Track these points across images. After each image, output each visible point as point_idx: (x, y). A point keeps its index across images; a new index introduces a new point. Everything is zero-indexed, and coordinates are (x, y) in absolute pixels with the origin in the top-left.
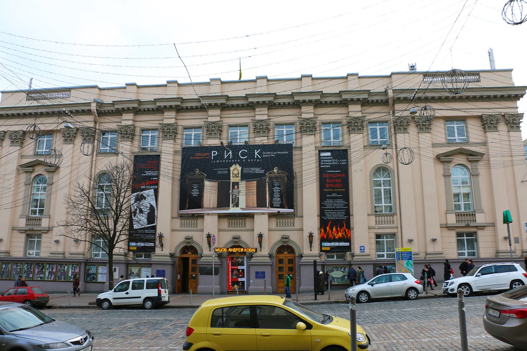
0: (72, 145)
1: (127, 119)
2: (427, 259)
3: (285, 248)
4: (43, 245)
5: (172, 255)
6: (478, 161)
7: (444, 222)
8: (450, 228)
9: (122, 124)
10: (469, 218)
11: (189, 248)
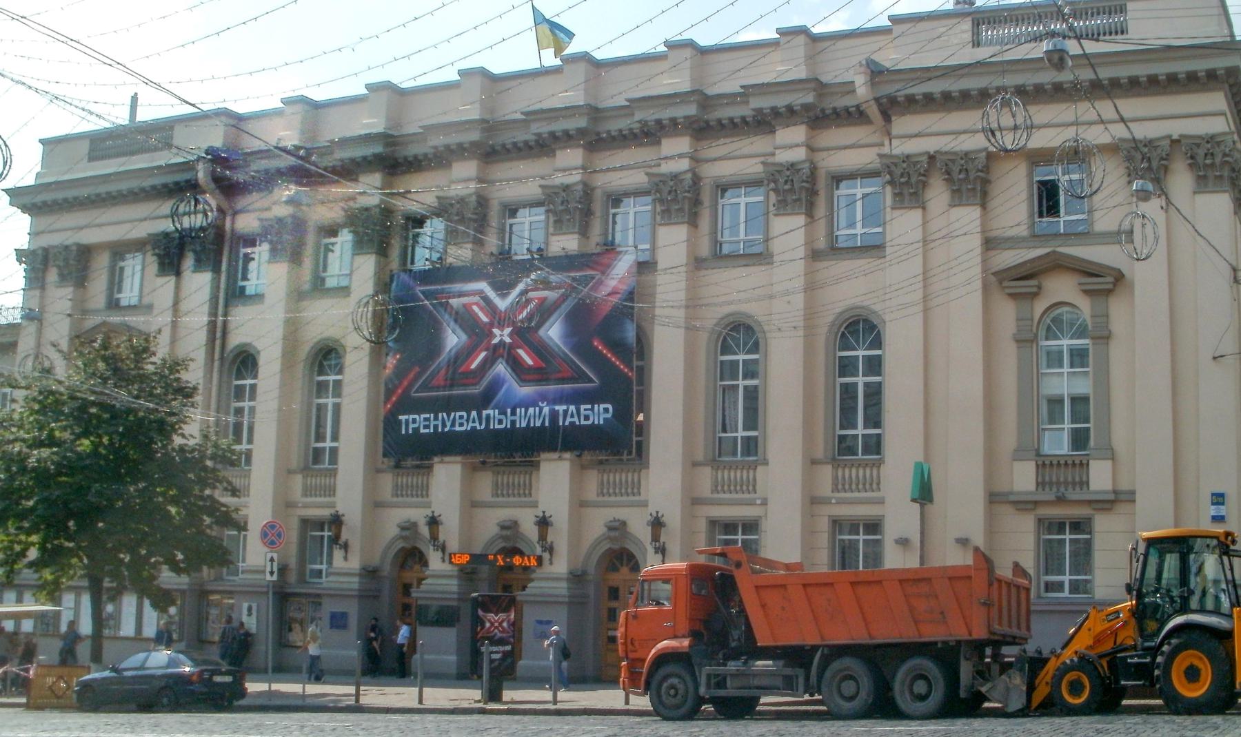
6: (1109, 292)
8: (1023, 505)
10: (1069, 474)
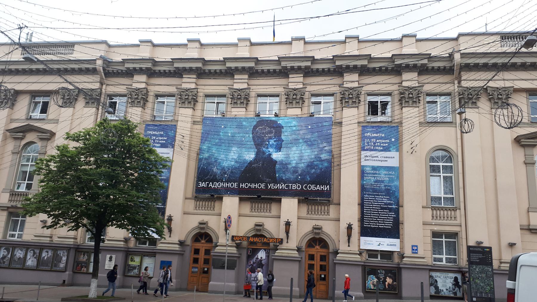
0: (72, 109)
1: (139, 82)
2: (502, 268)
3: (317, 240)
4: (27, 225)
5: (181, 243)
7: (525, 223)
11: (203, 235)
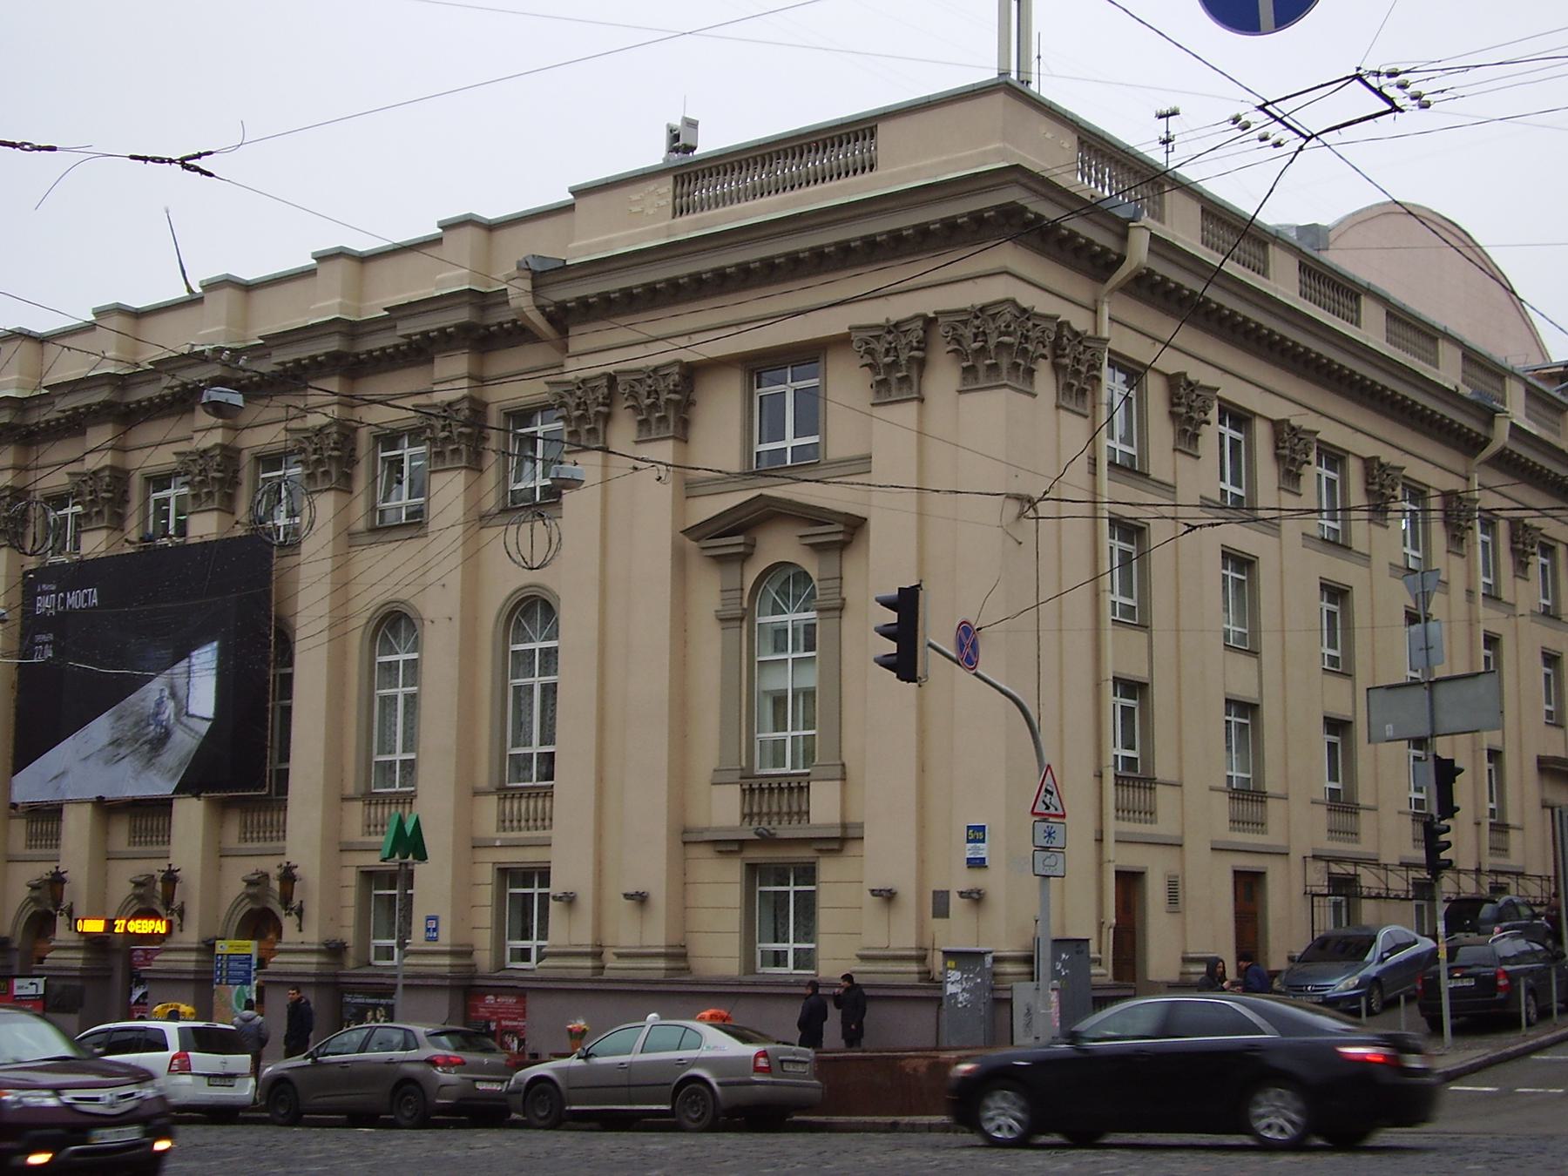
8: (726, 846)
9: (570, 377)
